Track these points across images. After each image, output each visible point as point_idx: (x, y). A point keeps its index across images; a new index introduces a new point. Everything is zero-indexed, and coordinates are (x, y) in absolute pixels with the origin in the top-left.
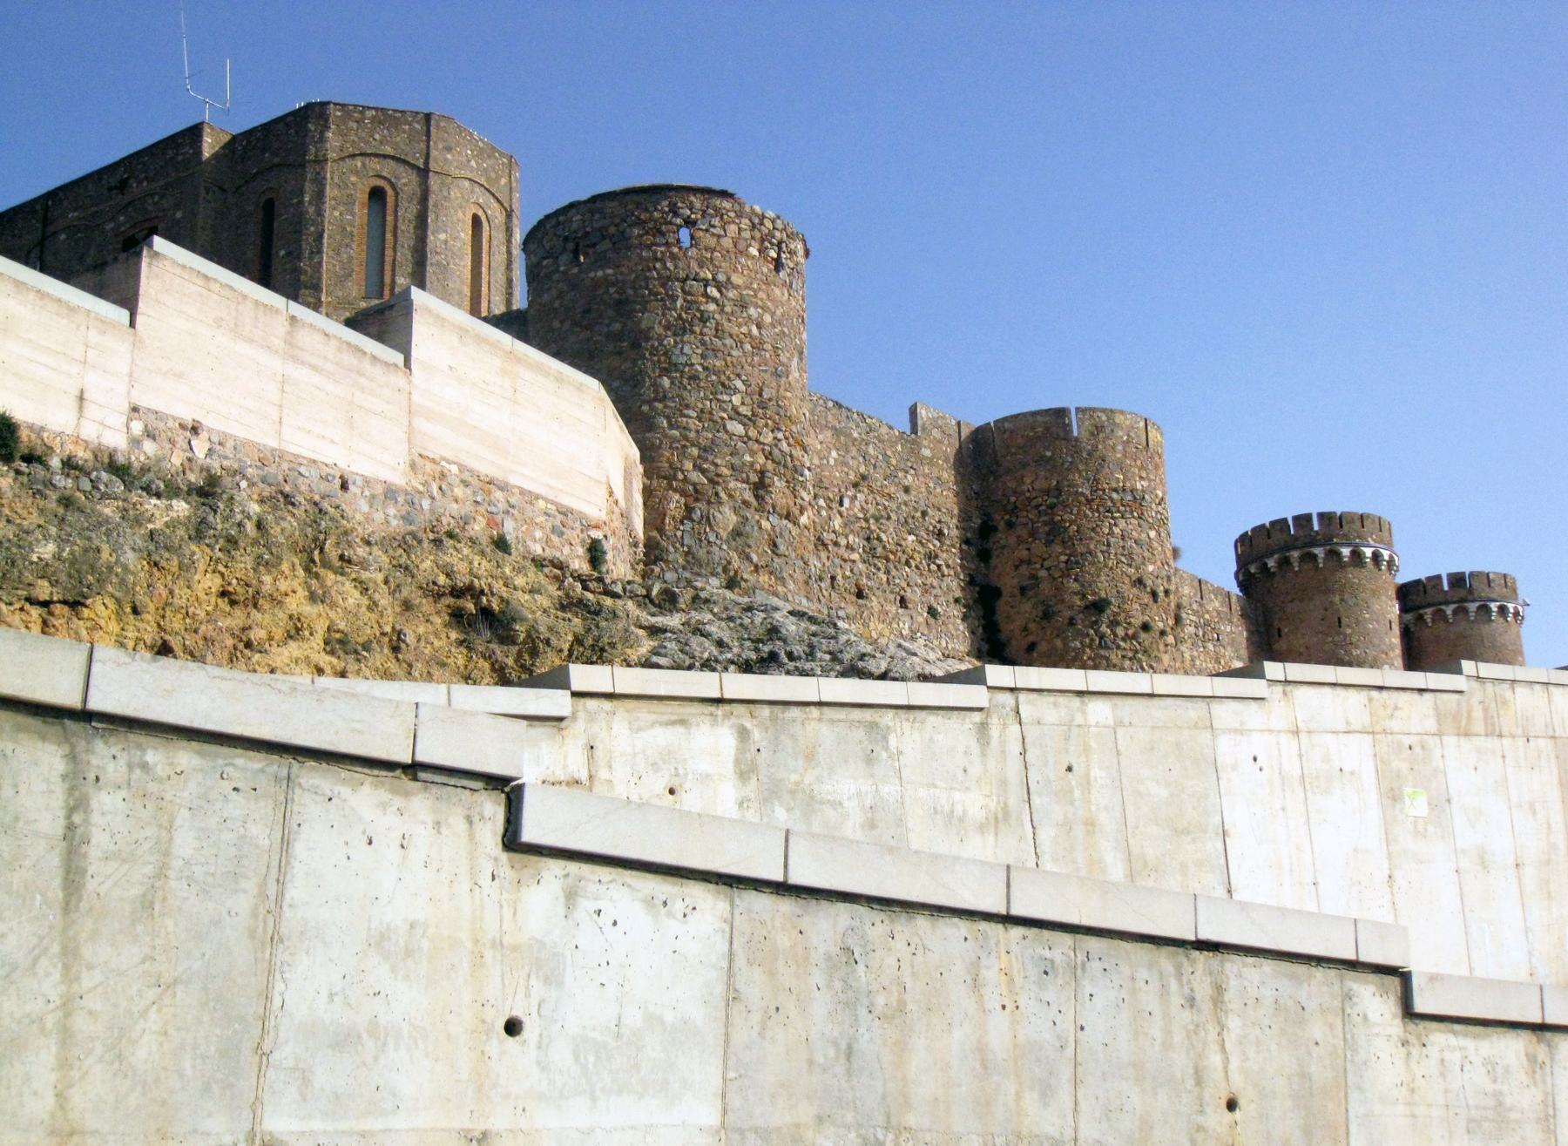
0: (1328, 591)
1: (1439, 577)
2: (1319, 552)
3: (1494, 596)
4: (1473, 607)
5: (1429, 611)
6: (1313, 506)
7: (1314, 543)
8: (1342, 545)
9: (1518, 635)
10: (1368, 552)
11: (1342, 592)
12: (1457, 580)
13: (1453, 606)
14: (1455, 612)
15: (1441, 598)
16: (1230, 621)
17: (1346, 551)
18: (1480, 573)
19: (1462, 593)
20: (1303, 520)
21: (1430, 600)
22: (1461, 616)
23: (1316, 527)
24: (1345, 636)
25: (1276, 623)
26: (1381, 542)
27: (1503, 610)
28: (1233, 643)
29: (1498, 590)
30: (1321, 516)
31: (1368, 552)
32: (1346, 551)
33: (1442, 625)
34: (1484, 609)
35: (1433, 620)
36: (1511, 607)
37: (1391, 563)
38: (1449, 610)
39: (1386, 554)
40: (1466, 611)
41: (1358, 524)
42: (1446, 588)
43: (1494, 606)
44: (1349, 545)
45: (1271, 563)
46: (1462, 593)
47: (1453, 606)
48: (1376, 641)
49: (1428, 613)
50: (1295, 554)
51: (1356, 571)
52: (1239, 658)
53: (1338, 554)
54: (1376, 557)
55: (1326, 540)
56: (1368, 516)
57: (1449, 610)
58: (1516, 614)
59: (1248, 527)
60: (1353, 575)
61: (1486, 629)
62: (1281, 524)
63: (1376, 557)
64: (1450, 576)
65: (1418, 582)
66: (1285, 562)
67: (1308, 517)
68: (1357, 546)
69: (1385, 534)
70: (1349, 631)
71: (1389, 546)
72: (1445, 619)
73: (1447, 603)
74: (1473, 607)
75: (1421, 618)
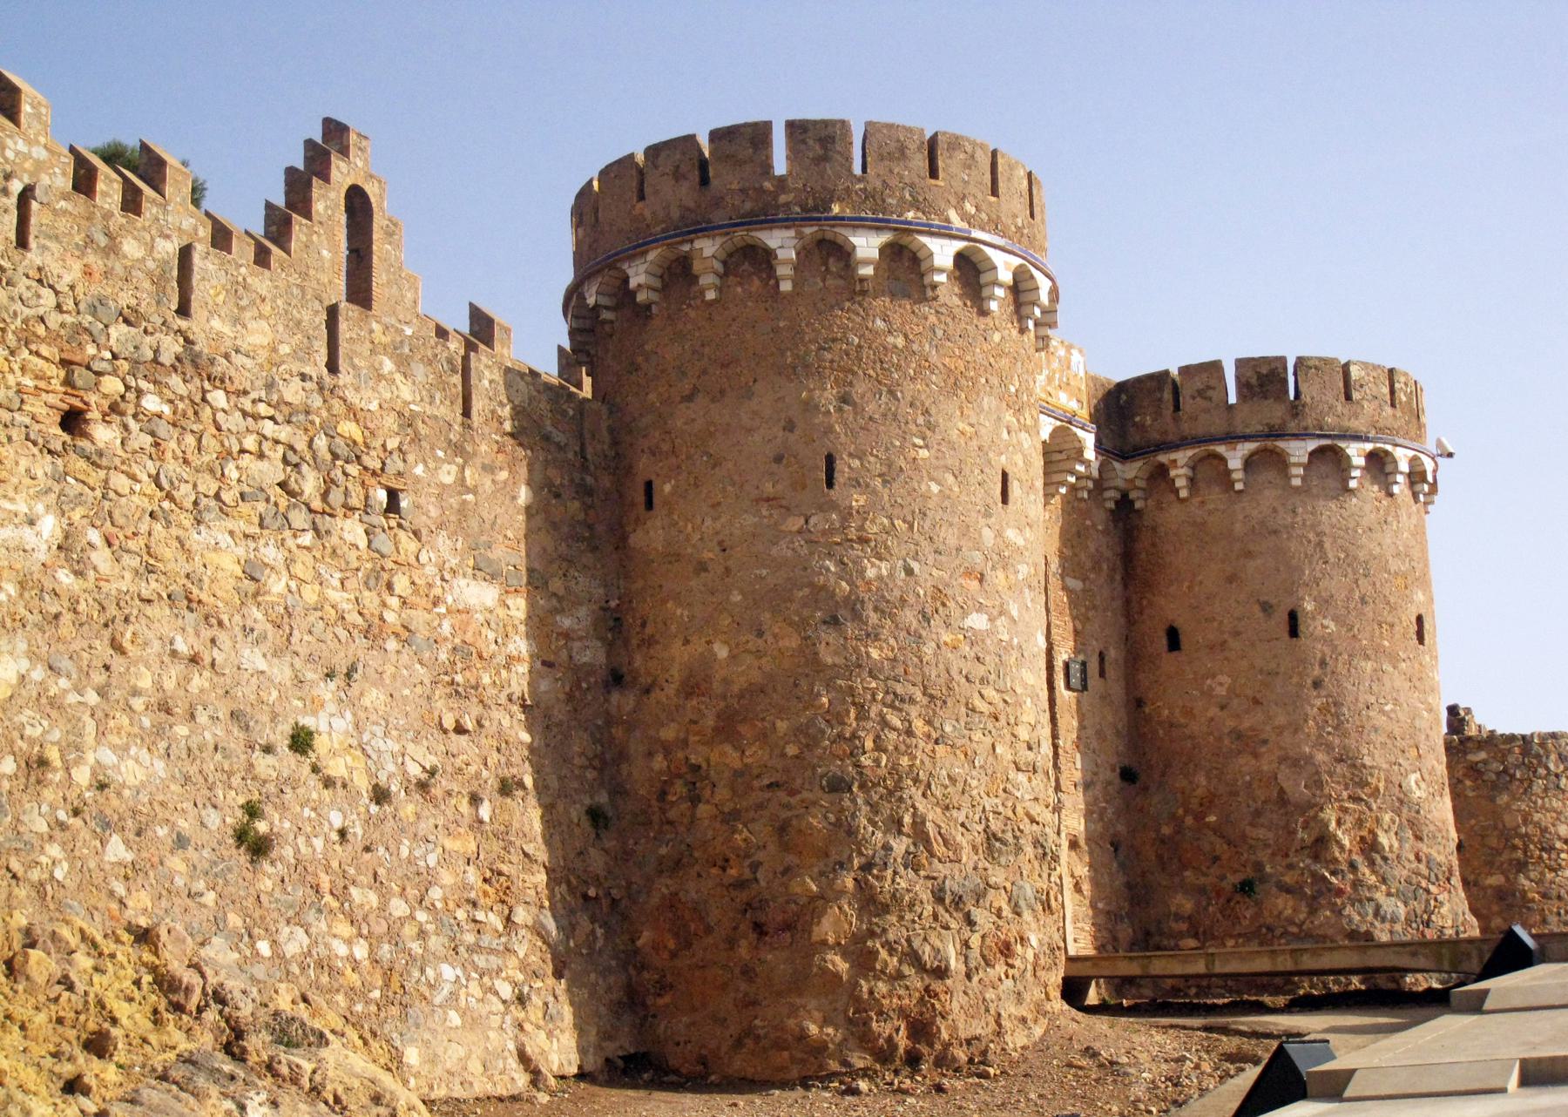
0: (801, 369)
1: (1215, 367)
2: (782, 243)
3: (1358, 425)
4: (1298, 451)
5: (1183, 456)
6: (777, 105)
7: (769, 219)
8: (858, 224)
9: (1419, 532)
10: (943, 253)
11: (846, 375)
12: (1263, 378)
13: (1250, 446)
14: (1248, 463)
15: (1217, 425)
16: (457, 449)
17: (867, 246)
18: (1326, 361)
19: (1273, 413)
20: (745, 141)
21: (1186, 428)
22: (1269, 475)
23: (780, 166)
24: (847, 515)
25: (645, 467)
26: (995, 225)
27: (1379, 463)
28: (460, 520)
29: (1370, 409)
30: (796, 129)
31: (943, 253)
32: (867, 246)
33: (1215, 496)
34: (1330, 458)
35: (1192, 481)
36: (1402, 457)
37: (1020, 290)
38: (1235, 458)
39: (1004, 266)
40: (1280, 462)
41: (920, 162)
42: (1232, 399)
43: (1356, 453)
44: (877, 226)
45: (639, 275)
46: (1273, 413)
47: (1250, 446)
48: (949, 536)
49: (1180, 462)
50: (708, 248)
51: (901, 311)
52: (485, 571)
53: (844, 253)
54: (970, 269)
55: (813, 209)
56: (955, 143)
57: (1235, 458)
58: (1416, 476)
59: (589, 170)
60: (889, 322)
61: (1329, 512)
62: (675, 154)
63: (970, 269)
64: (1241, 364)
65: (1161, 378)
66: (679, 273)
67: (758, 134)
68: (907, 230)
69: (1012, 204)
70: (858, 500)
71: (1025, 240)
72: (1224, 477)
73: (1231, 438)
74: (1298, 451)
75: (1161, 474)
